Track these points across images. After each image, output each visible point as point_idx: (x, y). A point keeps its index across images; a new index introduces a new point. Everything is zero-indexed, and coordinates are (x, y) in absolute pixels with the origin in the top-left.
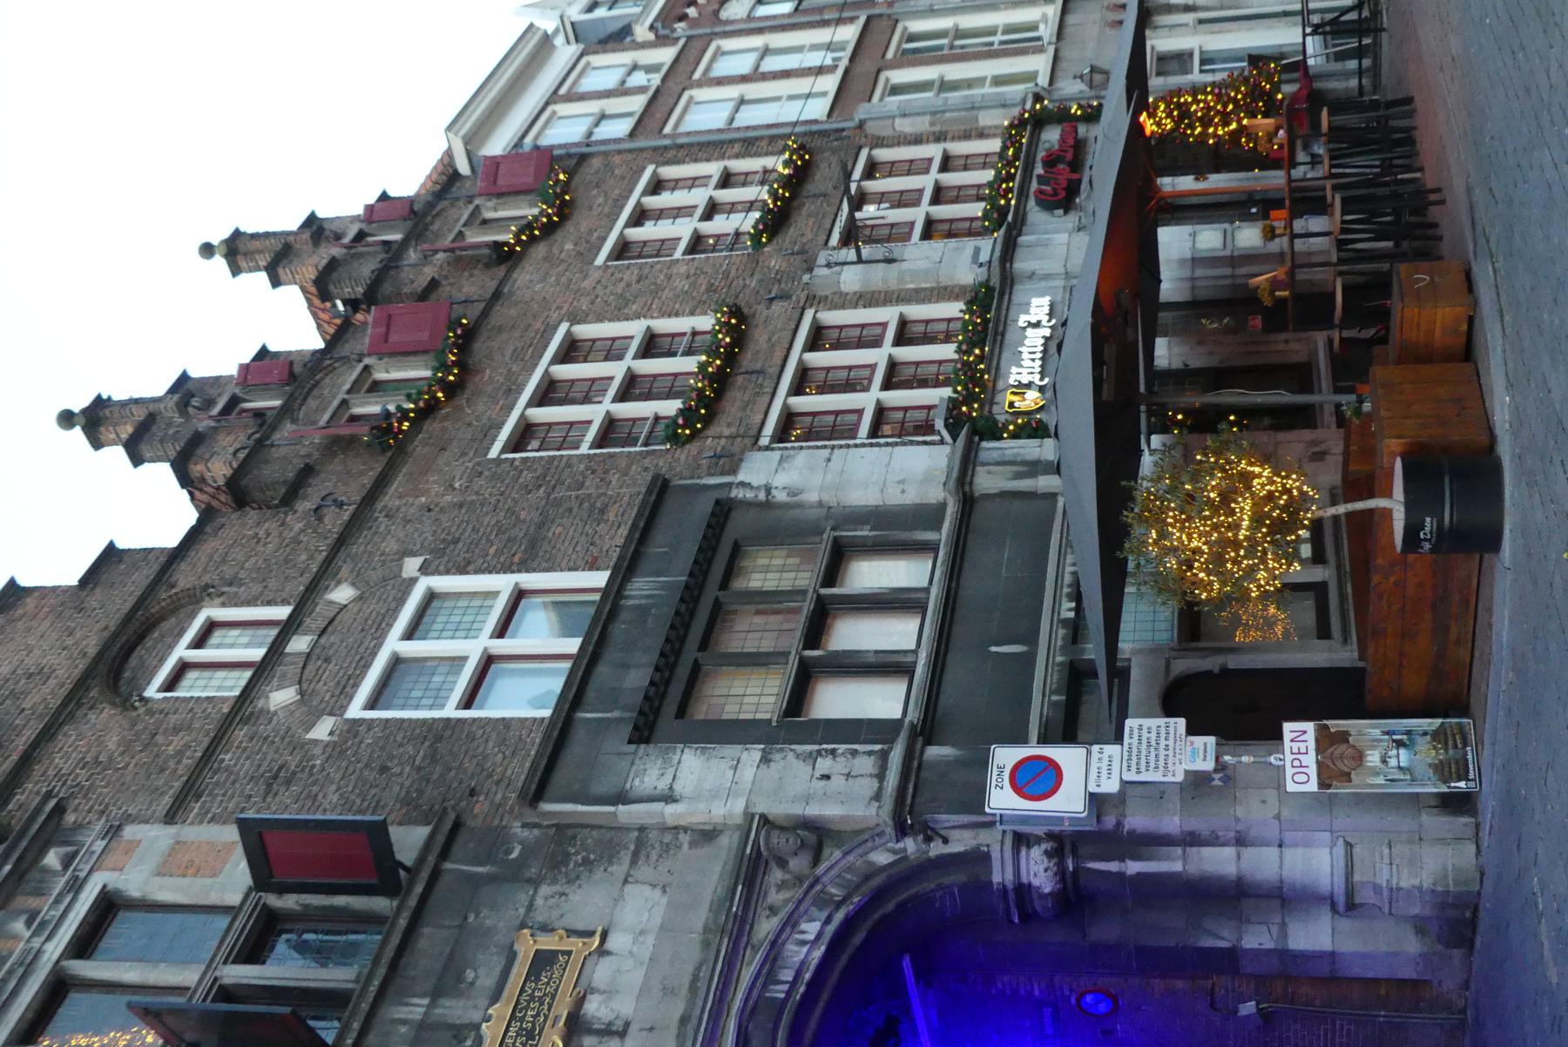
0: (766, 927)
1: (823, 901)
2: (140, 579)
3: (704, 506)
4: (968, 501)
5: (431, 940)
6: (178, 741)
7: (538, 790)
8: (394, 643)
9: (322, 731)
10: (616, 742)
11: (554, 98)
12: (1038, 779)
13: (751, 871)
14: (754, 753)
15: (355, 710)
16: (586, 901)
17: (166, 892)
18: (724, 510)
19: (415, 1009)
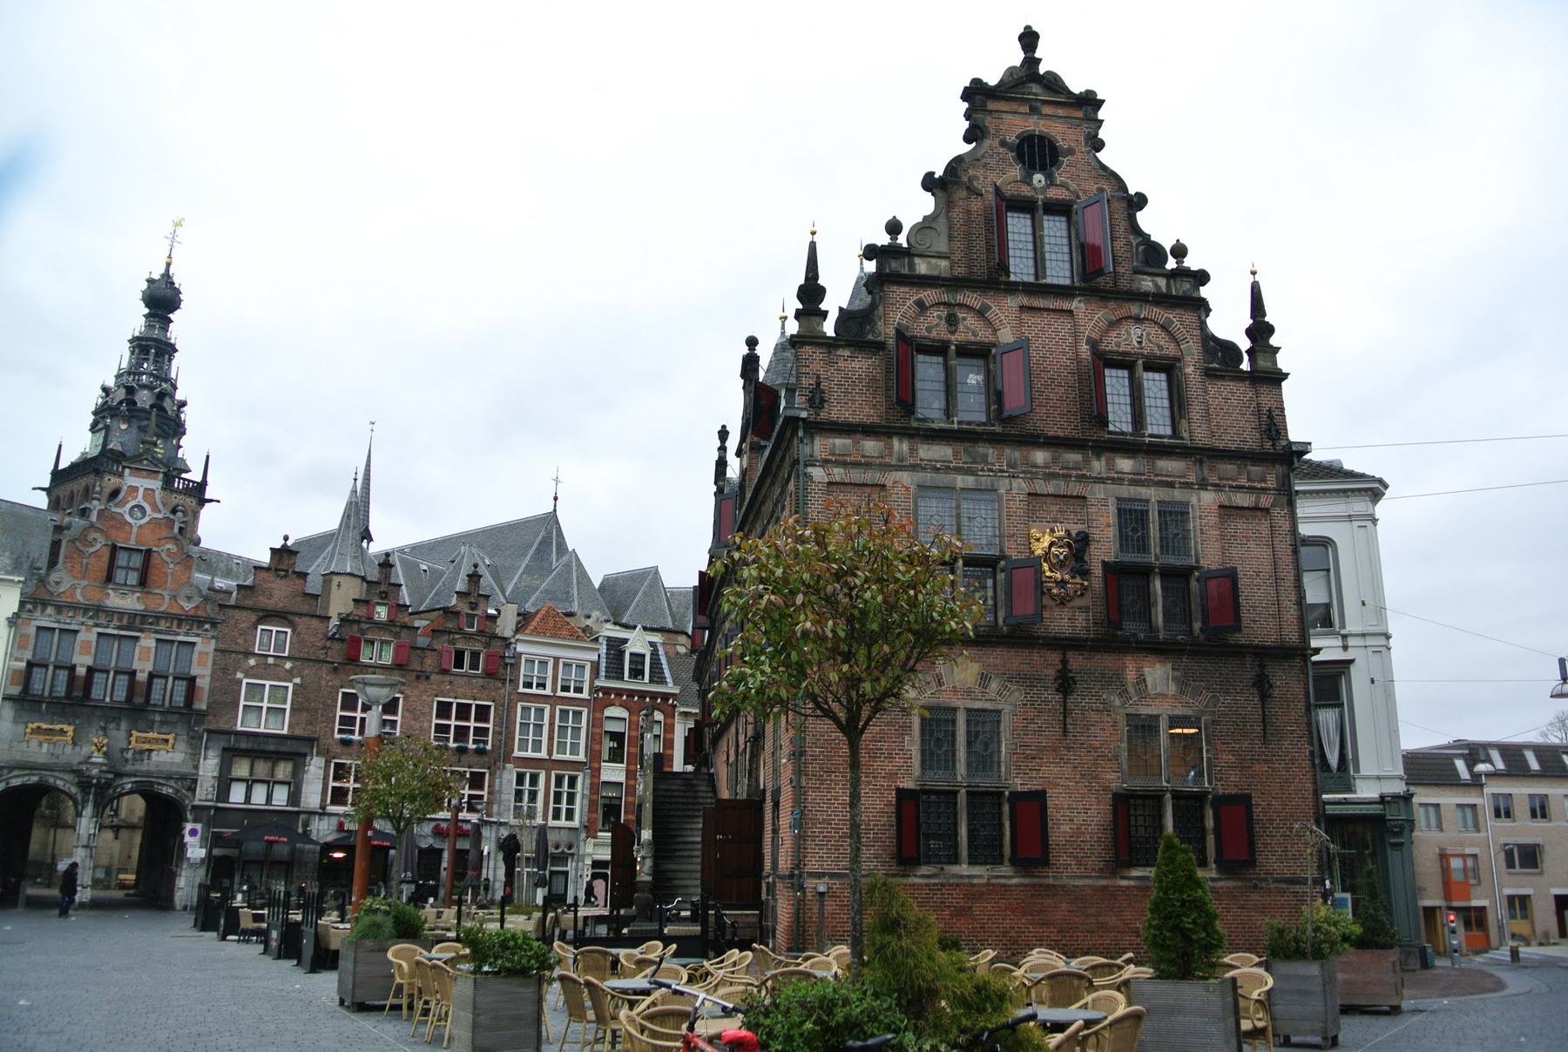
0: (172, 783)
1: (177, 791)
2: (305, 608)
3: (304, 750)
4: (298, 813)
5: (175, 717)
6: (240, 641)
7: (210, 732)
8: (268, 683)
9: (239, 675)
10: (223, 744)
11: (557, 659)
12: (193, 833)
13: (183, 778)
14: (216, 774)
15: (245, 681)
16: (181, 746)
17: (196, 656)
18: (305, 755)
19: (158, 718)
